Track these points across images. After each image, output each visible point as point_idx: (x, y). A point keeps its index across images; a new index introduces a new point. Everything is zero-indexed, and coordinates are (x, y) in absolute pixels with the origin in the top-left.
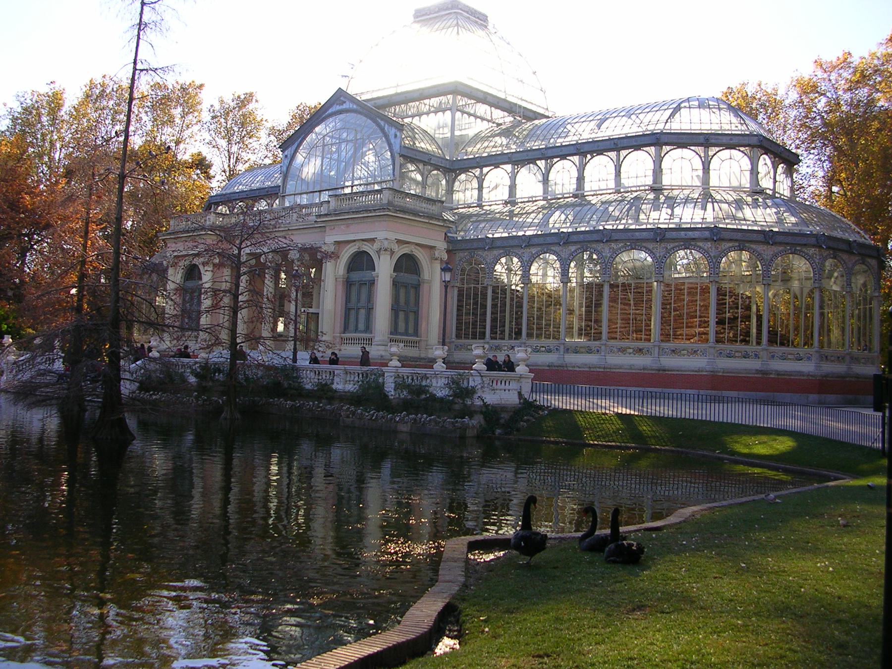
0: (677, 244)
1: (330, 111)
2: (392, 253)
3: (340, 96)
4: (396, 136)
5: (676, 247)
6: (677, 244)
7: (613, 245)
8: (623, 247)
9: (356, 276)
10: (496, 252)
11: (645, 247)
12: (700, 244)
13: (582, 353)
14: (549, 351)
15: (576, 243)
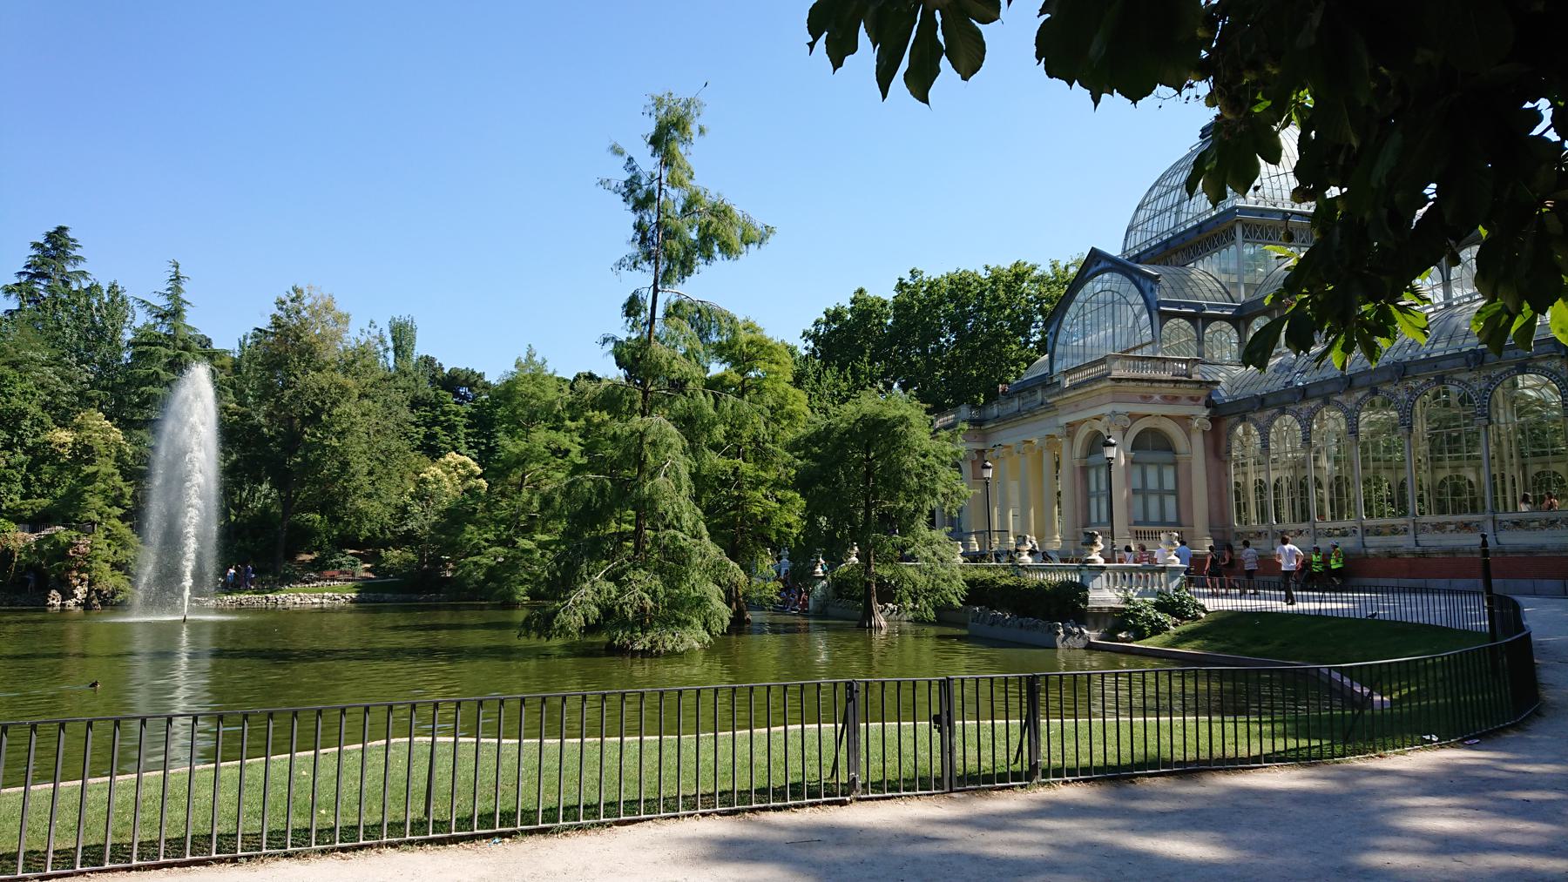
0: (1505, 369)
1: (1091, 272)
2: (1125, 431)
3: (1095, 255)
4: (1152, 290)
5: (1504, 373)
6: (1505, 369)
7: (1411, 384)
8: (1424, 384)
9: (1094, 459)
10: (1268, 413)
11: (1456, 380)
12: (1543, 364)
13: (1385, 535)
14: (1345, 534)
15: (1362, 388)
